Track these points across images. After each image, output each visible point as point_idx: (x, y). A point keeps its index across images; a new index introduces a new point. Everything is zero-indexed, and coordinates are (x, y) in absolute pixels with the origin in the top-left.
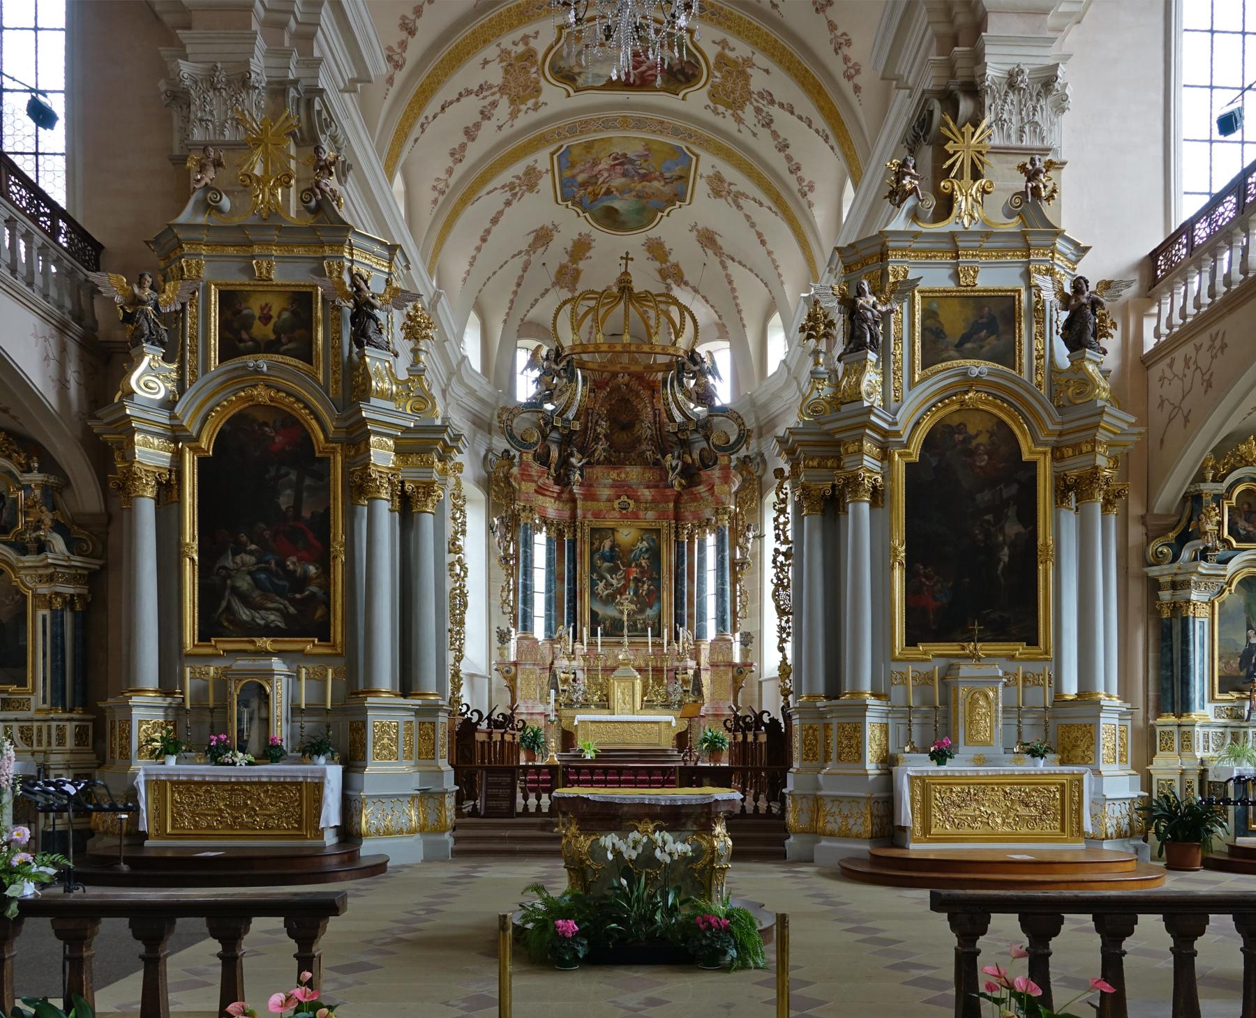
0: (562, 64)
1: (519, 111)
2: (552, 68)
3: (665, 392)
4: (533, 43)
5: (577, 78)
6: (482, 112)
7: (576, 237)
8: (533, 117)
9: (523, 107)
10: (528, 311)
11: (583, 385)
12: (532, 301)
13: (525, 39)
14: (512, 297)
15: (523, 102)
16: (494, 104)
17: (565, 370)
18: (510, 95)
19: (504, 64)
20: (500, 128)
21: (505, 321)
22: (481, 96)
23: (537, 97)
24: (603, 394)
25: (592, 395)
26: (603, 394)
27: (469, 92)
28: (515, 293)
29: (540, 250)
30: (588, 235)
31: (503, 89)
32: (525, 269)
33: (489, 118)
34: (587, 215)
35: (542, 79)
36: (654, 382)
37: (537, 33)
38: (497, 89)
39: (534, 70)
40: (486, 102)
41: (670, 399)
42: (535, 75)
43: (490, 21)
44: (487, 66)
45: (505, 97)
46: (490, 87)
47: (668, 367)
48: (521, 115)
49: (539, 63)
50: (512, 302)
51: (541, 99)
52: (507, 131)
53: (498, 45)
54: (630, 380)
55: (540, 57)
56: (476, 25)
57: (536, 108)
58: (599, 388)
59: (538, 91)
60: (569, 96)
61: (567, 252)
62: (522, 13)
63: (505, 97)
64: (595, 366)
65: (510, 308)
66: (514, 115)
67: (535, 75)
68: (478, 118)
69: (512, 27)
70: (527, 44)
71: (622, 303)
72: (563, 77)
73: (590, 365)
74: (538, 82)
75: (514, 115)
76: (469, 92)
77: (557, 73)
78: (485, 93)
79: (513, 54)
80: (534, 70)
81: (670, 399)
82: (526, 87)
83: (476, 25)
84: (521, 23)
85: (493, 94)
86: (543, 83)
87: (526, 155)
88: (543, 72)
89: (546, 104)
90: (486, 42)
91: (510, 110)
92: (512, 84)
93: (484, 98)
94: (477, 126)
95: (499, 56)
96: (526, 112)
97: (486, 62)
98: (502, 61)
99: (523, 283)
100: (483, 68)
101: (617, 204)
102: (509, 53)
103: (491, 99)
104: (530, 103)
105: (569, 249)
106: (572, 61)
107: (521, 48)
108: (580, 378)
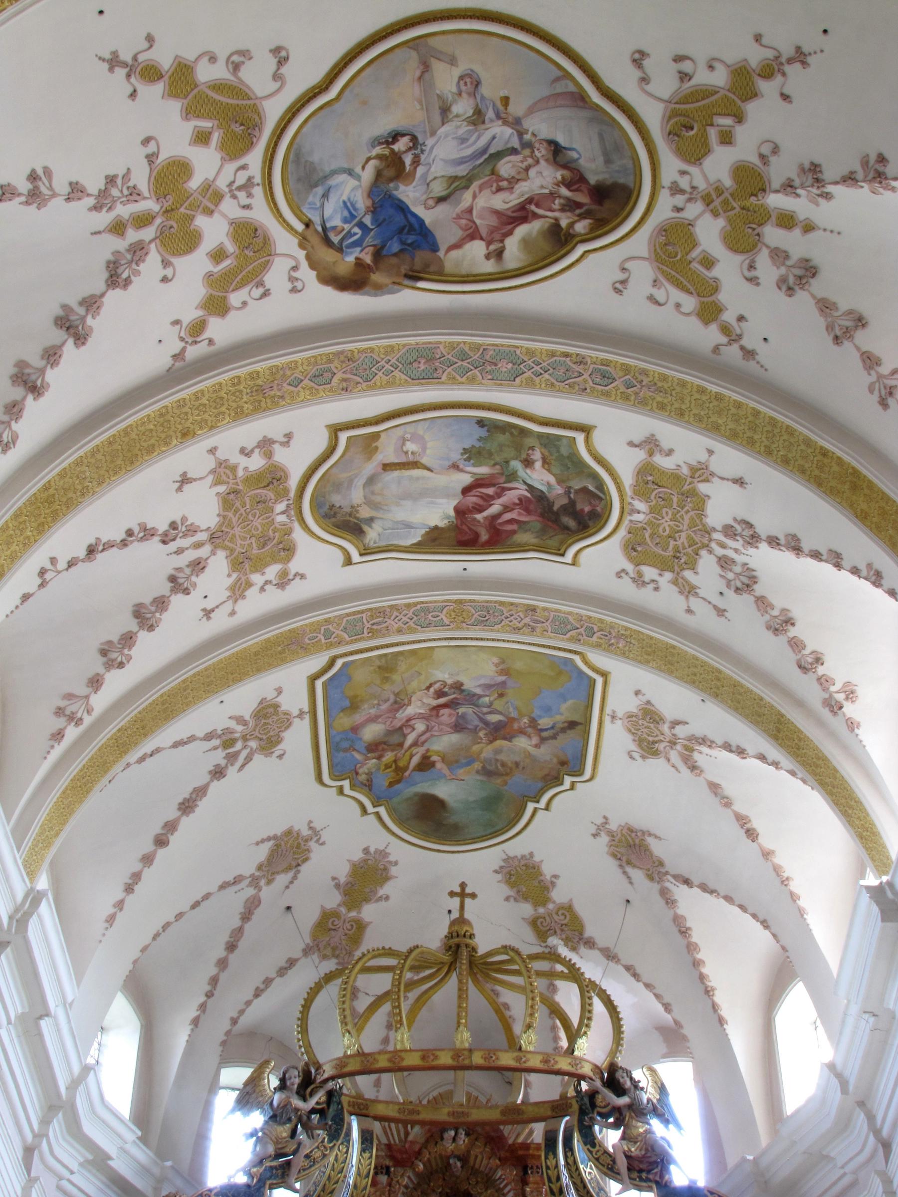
0: (337, 499)
1: (249, 585)
2: (316, 504)
3: (551, 1162)
4: (281, 456)
5: (365, 528)
6: (173, 579)
7: (358, 856)
8: (276, 599)
9: (257, 579)
10: (248, 1003)
11: (363, 1150)
12: (258, 982)
13: (266, 445)
14: (213, 971)
15: (259, 566)
16: (198, 566)
17: (322, 1112)
18: (232, 551)
19: (222, 489)
20: (208, 613)
21: (196, 1022)
22: (173, 546)
23: (289, 559)
24: (405, 1178)
25: (383, 1179)
26: (405, 1178)
27: (148, 533)
28: (222, 964)
29: (282, 879)
30: (383, 854)
31: (216, 538)
32: (246, 917)
33: (186, 592)
34: (382, 810)
35: (297, 526)
36: (526, 1146)
37: (289, 436)
38: (203, 536)
39: (280, 507)
40: (183, 560)
41: (565, 1179)
42: (282, 518)
43: (197, 396)
44: (186, 487)
45: (221, 554)
46: (192, 530)
47: (558, 1108)
48: (252, 593)
49: (292, 494)
50: (214, 981)
51: (294, 566)
52: (221, 622)
53: (212, 451)
54: (472, 1145)
55: (293, 483)
56: (169, 399)
57: (283, 581)
58: (399, 1163)
59: (288, 550)
60: (348, 562)
61: (337, 886)
62: (260, 390)
63: (221, 554)
64: (391, 1112)
65: (209, 995)
66: (238, 591)
67: (282, 518)
68: (165, 588)
69: (239, 415)
70: (269, 455)
71: (453, 979)
72: (337, 526)
73: (381, 1110)
74: (289, 532)
75: (238, 591)
76: (148, 533)
77: (326, 516)
78: (180, 543)
79: (240, 473)
80: (280, 507)
81: (565, 1179)
82: (264, 541)
83: (169, 399)
84: (258, 409)
85: (198, 545)
86: (299, 534)
87: (259, 670)
88: (301, 512)
89: (303, 576)
90: (186, 434)
91: (230, 581)
92: (237, 531)
93: (180, 551)
94: (161, 603)
95: (213, 471)
96: (262, 589)
97: (185, 480)
98: (217, 482)
99: (241, 944)
100: (179, 489)
101: (443, 790)
102: (234, 468)
103: (191, 555)
104: (272, 571)
105: (343, 880)
106: (357, 495)
107: (256, 463)
108: (355, 1134)
